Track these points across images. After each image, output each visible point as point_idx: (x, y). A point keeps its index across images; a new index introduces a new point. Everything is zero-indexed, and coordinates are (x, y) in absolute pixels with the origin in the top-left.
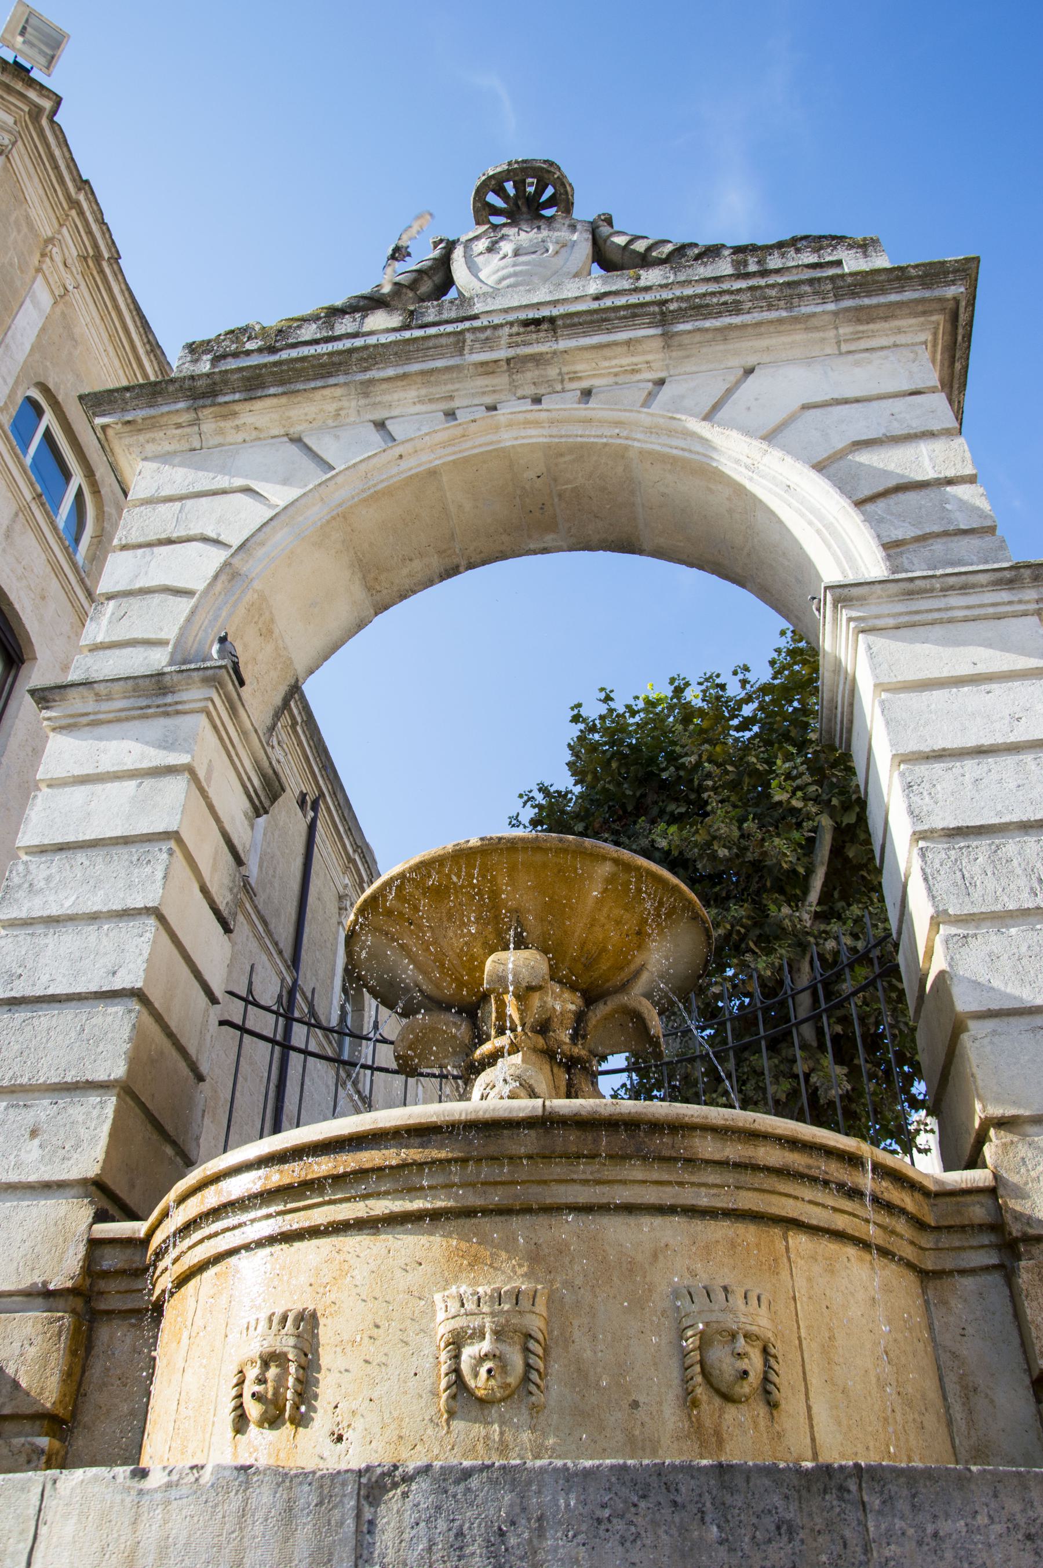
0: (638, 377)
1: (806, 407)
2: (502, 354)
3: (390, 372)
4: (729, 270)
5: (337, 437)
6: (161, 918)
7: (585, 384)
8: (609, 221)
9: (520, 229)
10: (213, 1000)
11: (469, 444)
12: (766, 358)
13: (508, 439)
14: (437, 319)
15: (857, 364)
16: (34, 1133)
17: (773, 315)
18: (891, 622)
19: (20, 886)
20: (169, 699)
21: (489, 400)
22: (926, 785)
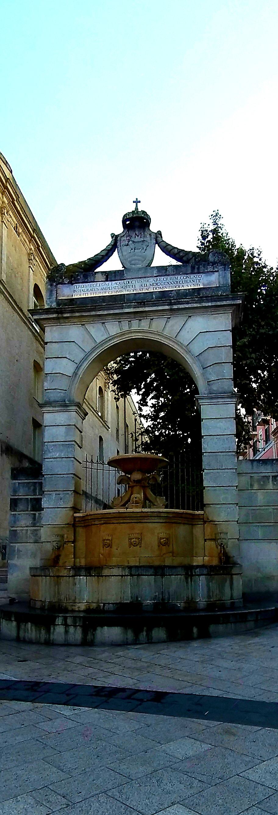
0: (165, 317)
1: (200, 332)
2: (132, 310)
3: (105, 312)
4: (190, 272)
5: (93, 327)
6: (74, 458)
7: (152, 318)
8: (161, 235)
9: (136, 234)
10: (80, 463)
11: (125, 337)
12: (194, 314)
13: (134, 336)
14: (115, 279)
15: (214, 318)
16: (61, 499)
17: (195, 305)
18: (207, 404)
19: (47, 450)
20: (68, 408)
21: (129, 320)
22: (207, 442)
